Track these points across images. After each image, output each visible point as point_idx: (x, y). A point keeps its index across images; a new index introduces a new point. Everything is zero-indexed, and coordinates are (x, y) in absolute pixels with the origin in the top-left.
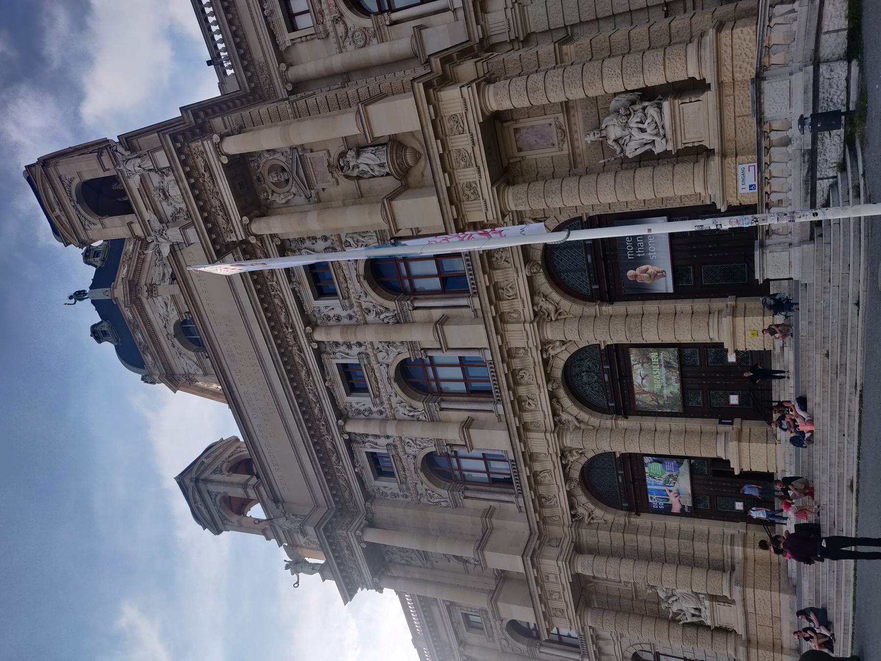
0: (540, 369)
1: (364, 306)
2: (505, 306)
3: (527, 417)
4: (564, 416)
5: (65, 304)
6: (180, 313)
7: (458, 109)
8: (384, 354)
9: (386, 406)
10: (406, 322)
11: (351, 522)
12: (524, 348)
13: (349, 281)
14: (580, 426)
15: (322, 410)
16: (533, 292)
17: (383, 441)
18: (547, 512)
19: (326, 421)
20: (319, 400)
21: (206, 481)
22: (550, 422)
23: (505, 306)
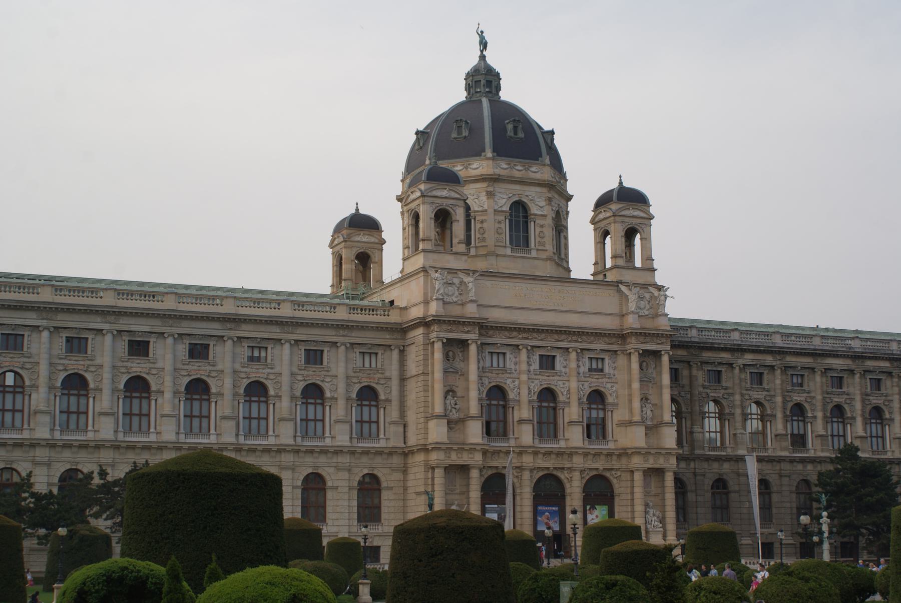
0: (561, 466)
1: (586, 384)
2: (590, 457)
3: (540, 456)
4: (535, 472)
5: (479, 24)
6: (536, 215)
7: (671, 462)
8: (562, 386)
10: (579, 403)
12: (571, 460)
13: (596, 380)
15: (536, 339)
17: (513, 367)
19: (531, 339)
20: (541, 340)
23: (590, 457)
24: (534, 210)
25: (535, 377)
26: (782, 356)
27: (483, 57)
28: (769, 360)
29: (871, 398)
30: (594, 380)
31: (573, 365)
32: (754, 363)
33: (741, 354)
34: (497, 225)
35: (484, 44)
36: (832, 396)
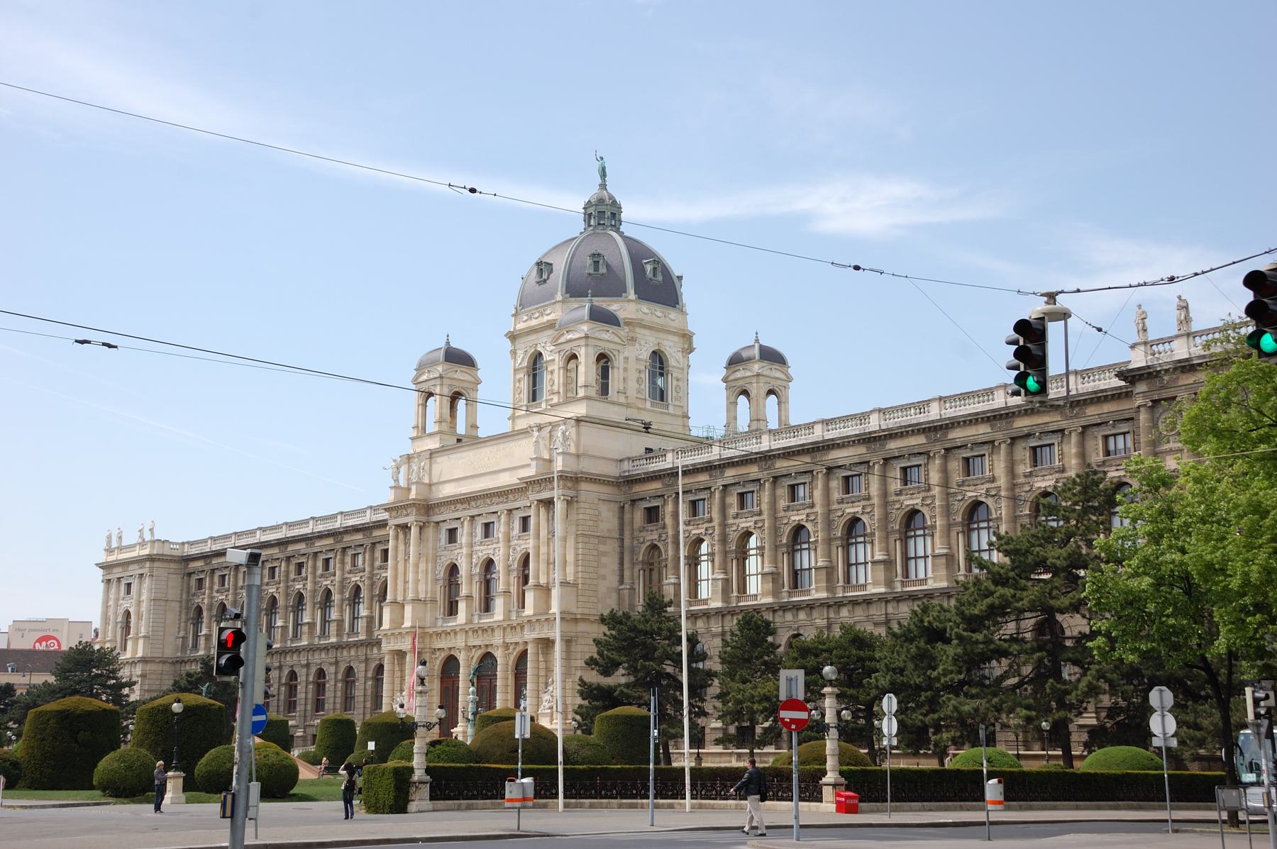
4: (473, 650)
6: (547, 362)
9: (478, 548)
11: (421, 515)
14: (469, 659)
16: (517, 644)
18: (434, 637)
19: (468, 509)
20: (477, 507)
21: (442, 385)
22: (470, 644)
24: (547, 357)
25: (478, 548)
26: (770, 462)
27: (603, 186)
28: (753, 471)
29: (902, 498)
30: (524, 542)
31: (502, 529)
32: (737, 480)
33: (721, 472)
34: (517, 384)
35: (603, 173)
36: (845, 505)
